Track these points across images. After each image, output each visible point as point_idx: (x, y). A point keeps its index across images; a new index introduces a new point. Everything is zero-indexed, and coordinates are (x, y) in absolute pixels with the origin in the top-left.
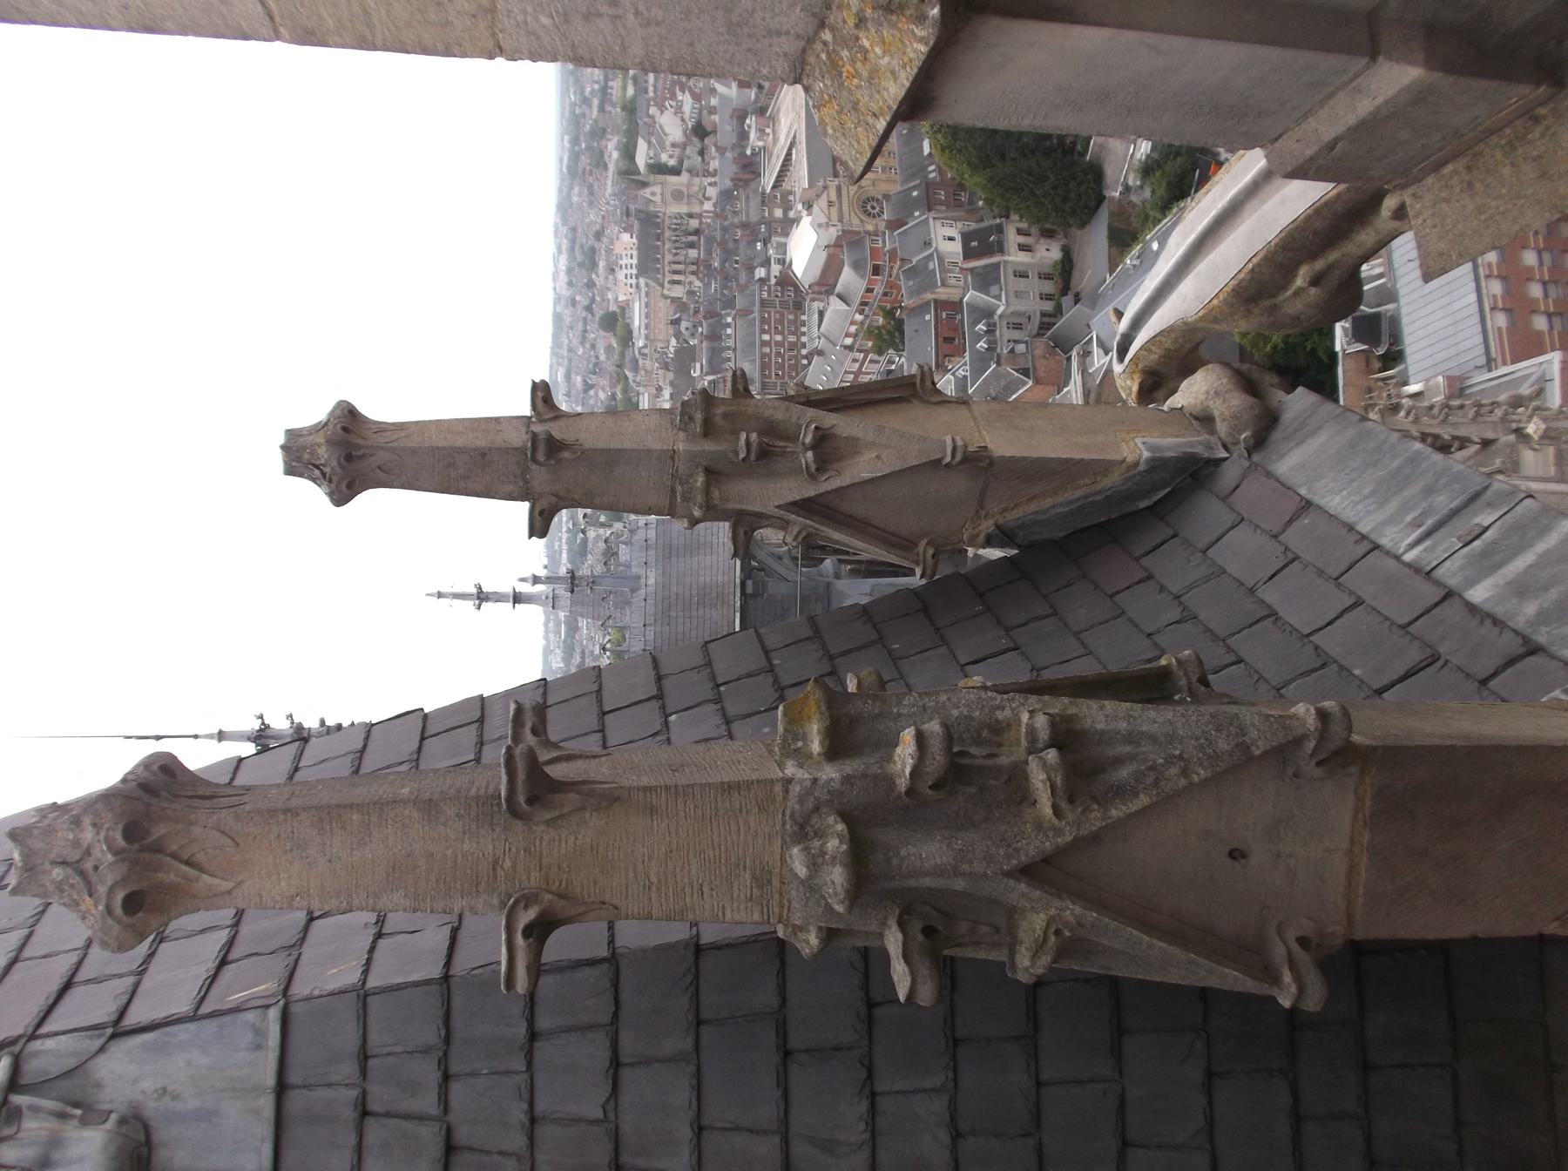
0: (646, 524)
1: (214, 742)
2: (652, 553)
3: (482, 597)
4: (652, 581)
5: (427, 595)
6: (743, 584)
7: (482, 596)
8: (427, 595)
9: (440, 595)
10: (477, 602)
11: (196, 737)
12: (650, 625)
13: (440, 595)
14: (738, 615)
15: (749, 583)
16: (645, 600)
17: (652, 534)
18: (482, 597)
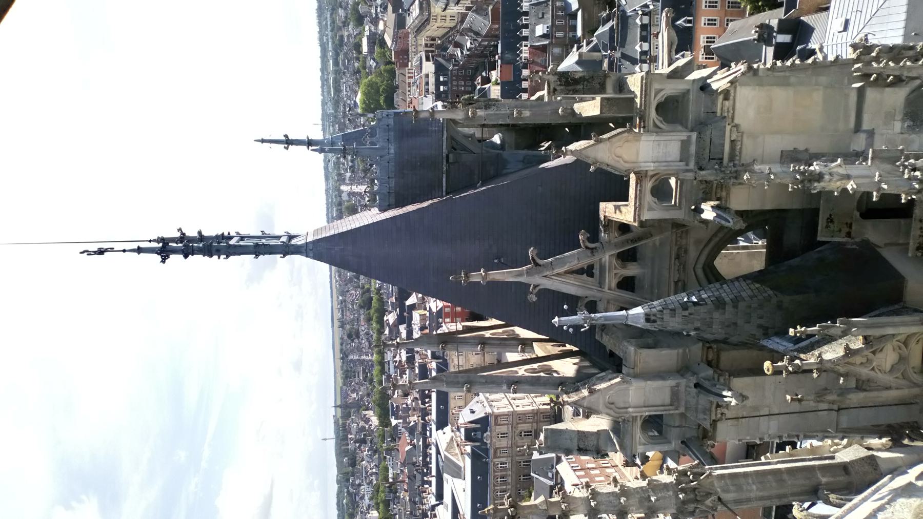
0: (387, 115)
1: (136, 254)
2: (392, 133)
3: (288, 142)
4: (392, 151)
5: (255, 141)
6: (447, 156)
7: (289, 142)
8: (255, 141)
9: (263, 141)
10: (286, 146)
11: (124, 251)
12: (392, 178)
13: (263, 141)
14: (444, 175)
15: (451, 156)
16: (388, 162)
17: (391, 122)
18: (288, 142)
